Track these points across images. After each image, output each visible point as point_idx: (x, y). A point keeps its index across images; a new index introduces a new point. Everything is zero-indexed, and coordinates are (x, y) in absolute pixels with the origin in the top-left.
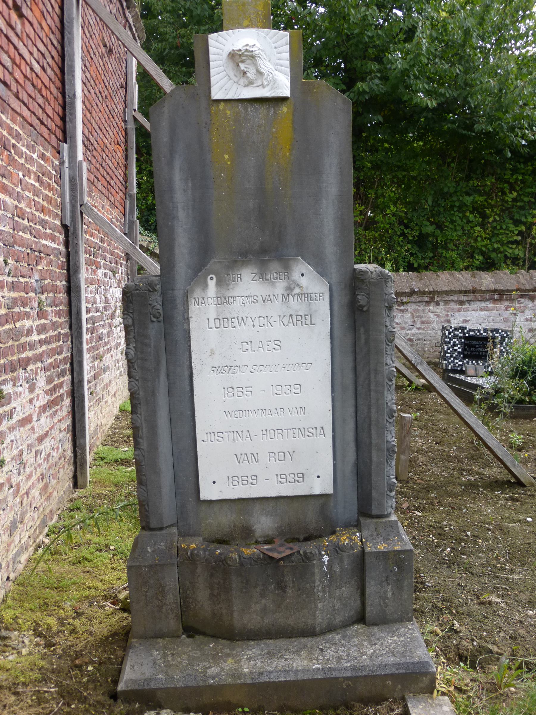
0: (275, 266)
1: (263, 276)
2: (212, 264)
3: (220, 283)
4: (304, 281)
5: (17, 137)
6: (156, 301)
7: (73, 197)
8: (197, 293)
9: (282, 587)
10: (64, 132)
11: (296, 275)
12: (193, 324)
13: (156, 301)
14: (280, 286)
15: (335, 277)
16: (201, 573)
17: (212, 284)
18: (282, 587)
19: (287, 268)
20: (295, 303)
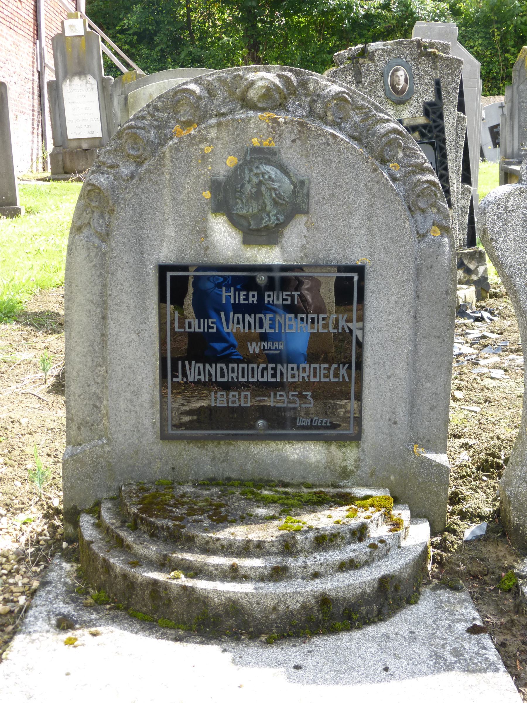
0: (83, 76)
1: (80, 79)
2: (68, 76)
3: (70, 81)
4: (90, 80)
5: (20, 42)
6: (54, 86)
7: (41, 61)
8: (64, 83)
9: (87, 158)
10: (37, 35)
11: (88, 78)
12: (64, 91)
13: (54, 86)
14: (85, 81)
15: (98, 79)
16: (67, 156)
17: (68, 81)
18: (87, 158)
19: (86, 77)
20: (88, 86)
